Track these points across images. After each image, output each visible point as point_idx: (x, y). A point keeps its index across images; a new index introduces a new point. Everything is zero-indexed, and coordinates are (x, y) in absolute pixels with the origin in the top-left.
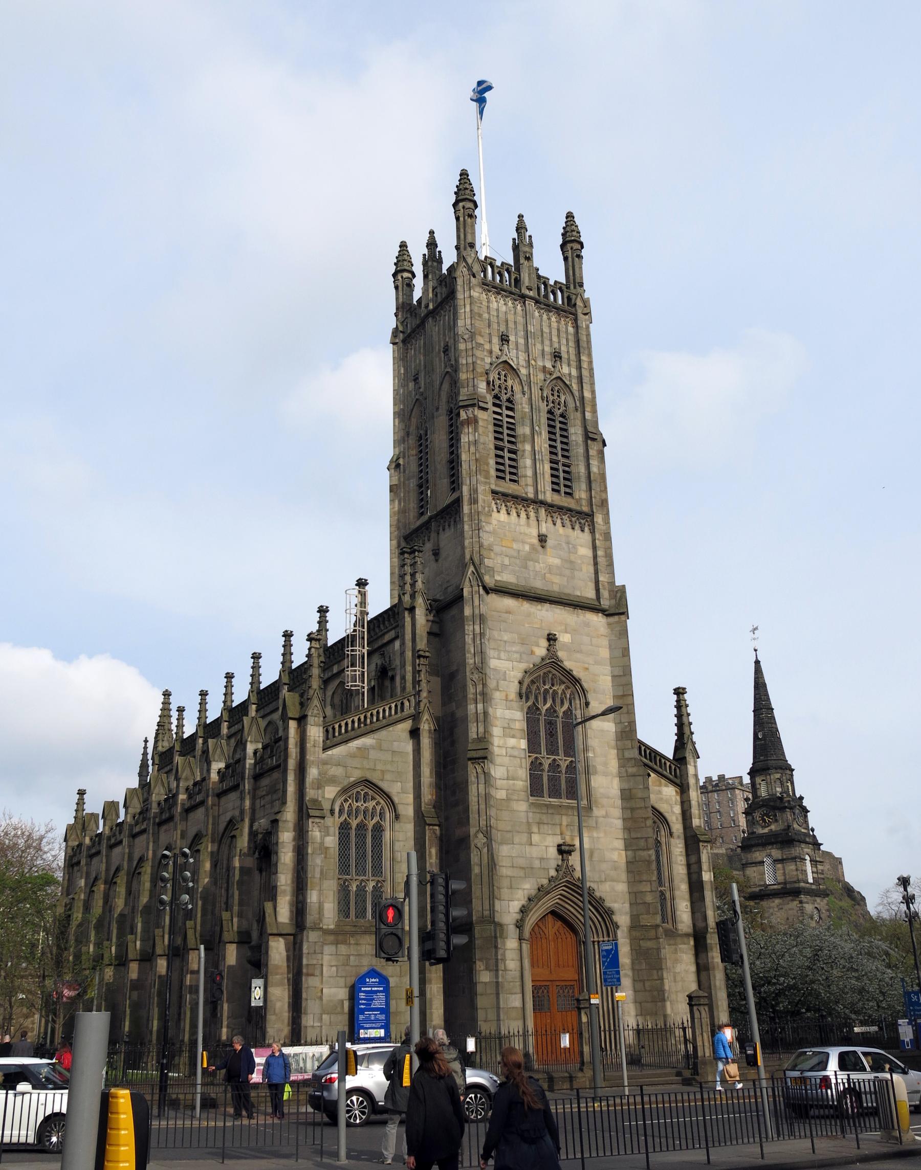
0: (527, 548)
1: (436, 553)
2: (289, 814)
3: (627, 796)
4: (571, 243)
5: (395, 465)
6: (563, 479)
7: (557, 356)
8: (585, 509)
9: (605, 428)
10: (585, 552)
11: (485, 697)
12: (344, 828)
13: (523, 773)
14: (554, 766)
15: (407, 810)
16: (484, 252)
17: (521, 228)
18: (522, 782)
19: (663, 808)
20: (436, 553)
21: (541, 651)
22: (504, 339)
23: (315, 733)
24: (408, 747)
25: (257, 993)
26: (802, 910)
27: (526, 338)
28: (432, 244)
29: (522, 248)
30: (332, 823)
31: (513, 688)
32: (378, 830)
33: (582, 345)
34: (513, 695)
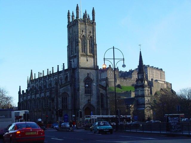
0: (85, 62)
1: (74, 61)
2: (56, 97)
3: (97, 93)
5: (68, 47)
7: (90, 32)
10: (93, 61)
11: (79, 82)
12: (62, 98)
13: (84, 91)
14: (88, 90)
15: (70, 95)
18: (84, 92)
19: (104, 93)
20: (74, 61)
21: (87, 76)
22: (83, 31)
23: (59, 87)
24: (70, 88)
25: (53, 117)
26: (144, 99)
27: (86, 30)
30: (61, 97)
31: (83, 81)
32: (66, 98)
33: (94, 30)
34: (83, 81)
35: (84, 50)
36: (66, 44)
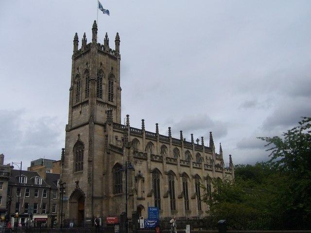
4: (118, 41)
6: (111, 96)
7: (112, 69)
8: (115, 105)
9: (121, 86)
16: (98, 42)
17: (106, 36)
28: (85, 36)
29: (107, 41)
35: (99, 93)
36: (68, 83)
